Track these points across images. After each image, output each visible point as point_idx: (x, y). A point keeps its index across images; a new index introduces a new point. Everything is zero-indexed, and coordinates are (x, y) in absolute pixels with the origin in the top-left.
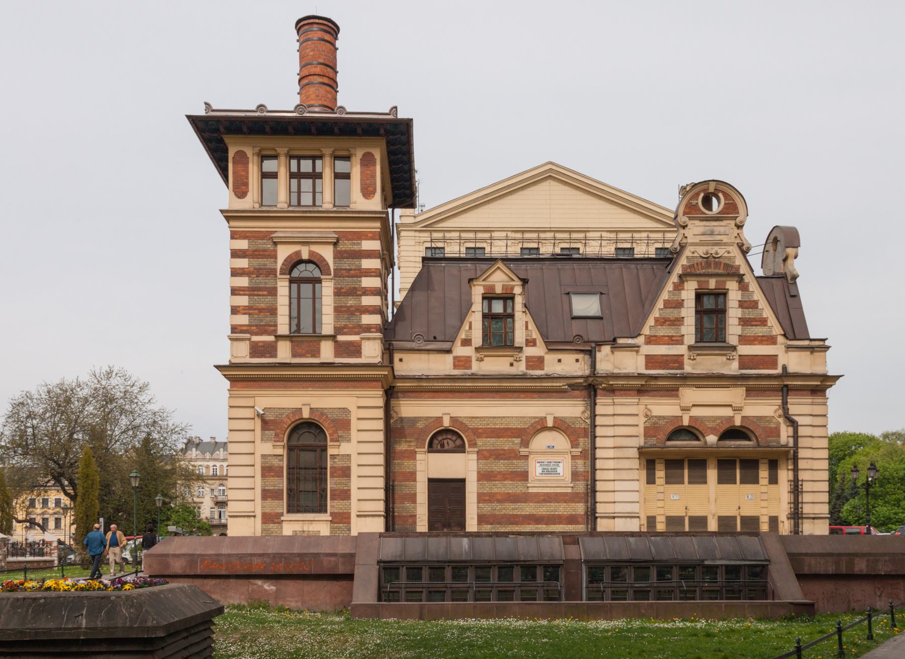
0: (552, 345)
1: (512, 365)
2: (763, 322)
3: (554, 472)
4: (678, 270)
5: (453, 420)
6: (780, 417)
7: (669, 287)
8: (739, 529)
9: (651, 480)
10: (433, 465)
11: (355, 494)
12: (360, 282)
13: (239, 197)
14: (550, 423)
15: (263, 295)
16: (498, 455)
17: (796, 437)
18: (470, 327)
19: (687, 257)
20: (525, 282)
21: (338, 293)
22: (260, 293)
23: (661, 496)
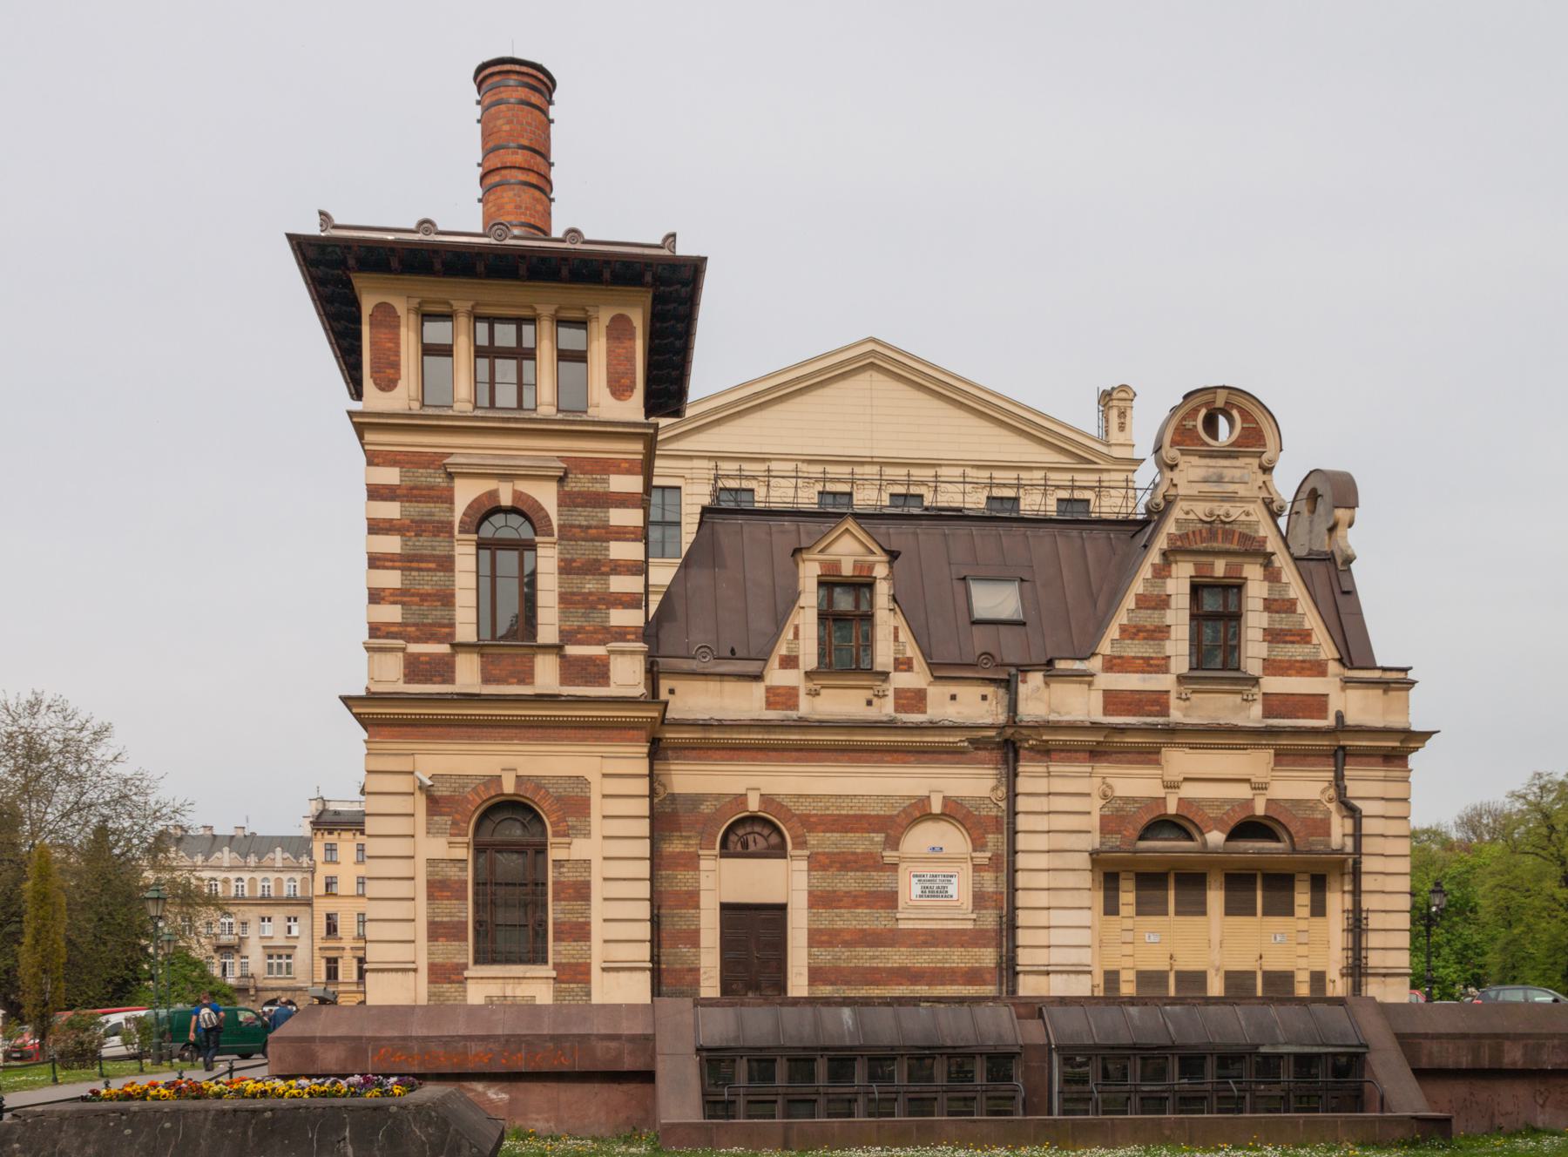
0: (942, 670)
1: (869, 703)
2: (1304, 637)
3: (942, 892)
4: (1161, 543)
5: (766, 799)
6: (1330, 800)
7: (1146, 571)
8: (1259, 993)
9: (1111, 908)
10: (727, 880)
11: (598, 930)
12: (607, 549)
13: (382, 389)
14: (936, 808)
15: (429, 570)
16: (845, 862)
17: (1357, 835)
19: (1177, 521)
20: (893, 555)
21: (566, 568)
22: (423, 565)
23: (1128, 937)
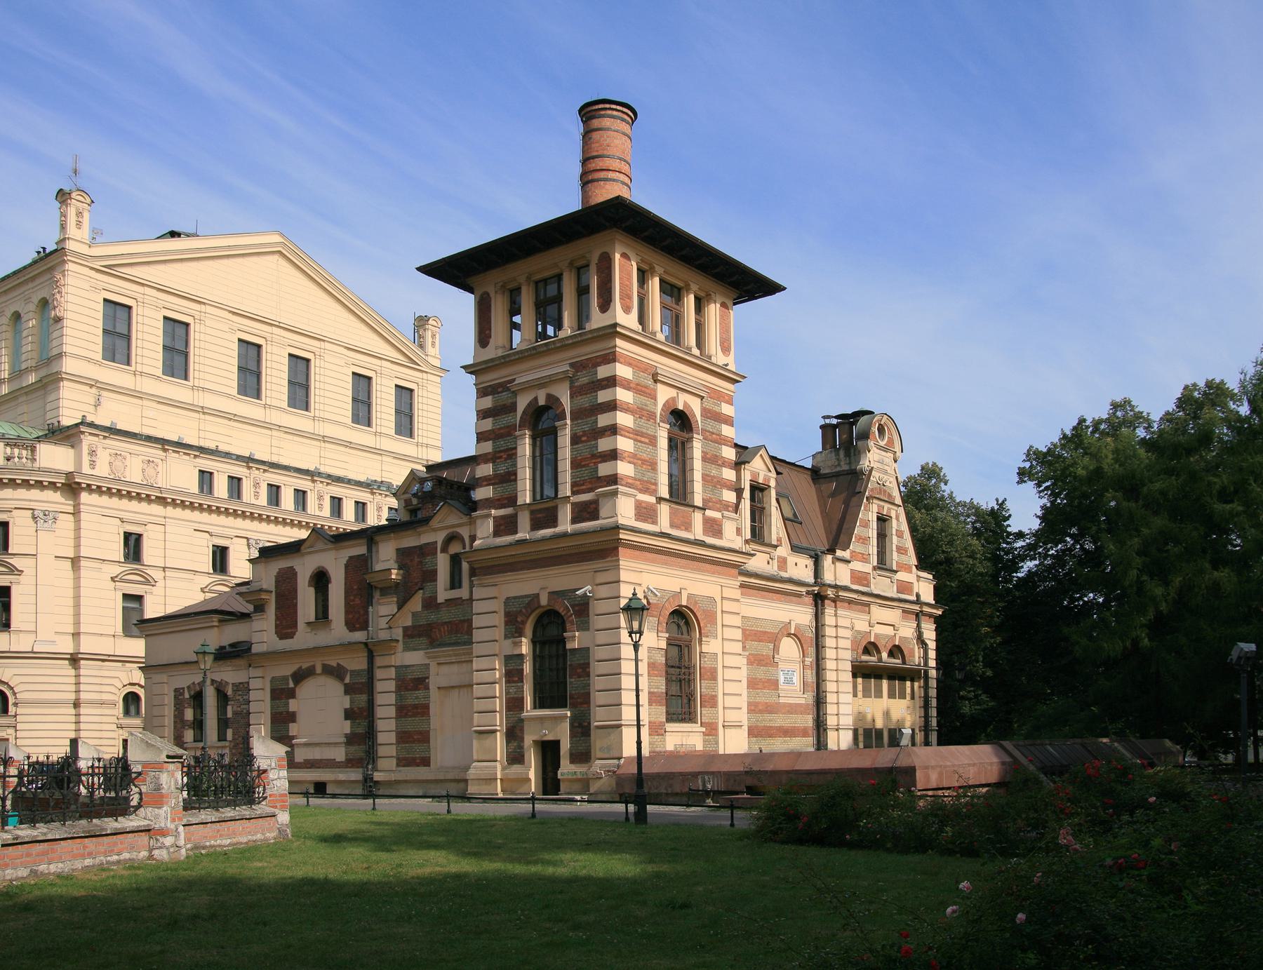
0: (795, 548)
20: (778, 473)
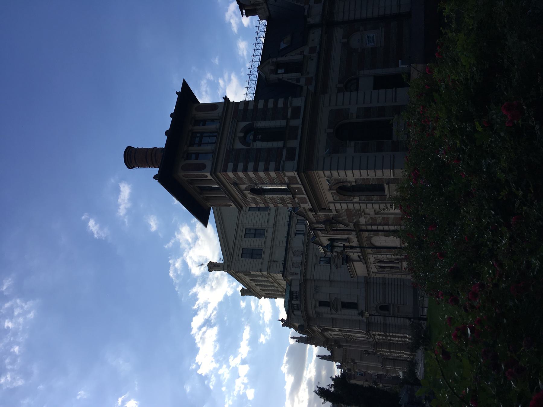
1: (312, 60)
18: (291, 79)
21: (264, 119)
